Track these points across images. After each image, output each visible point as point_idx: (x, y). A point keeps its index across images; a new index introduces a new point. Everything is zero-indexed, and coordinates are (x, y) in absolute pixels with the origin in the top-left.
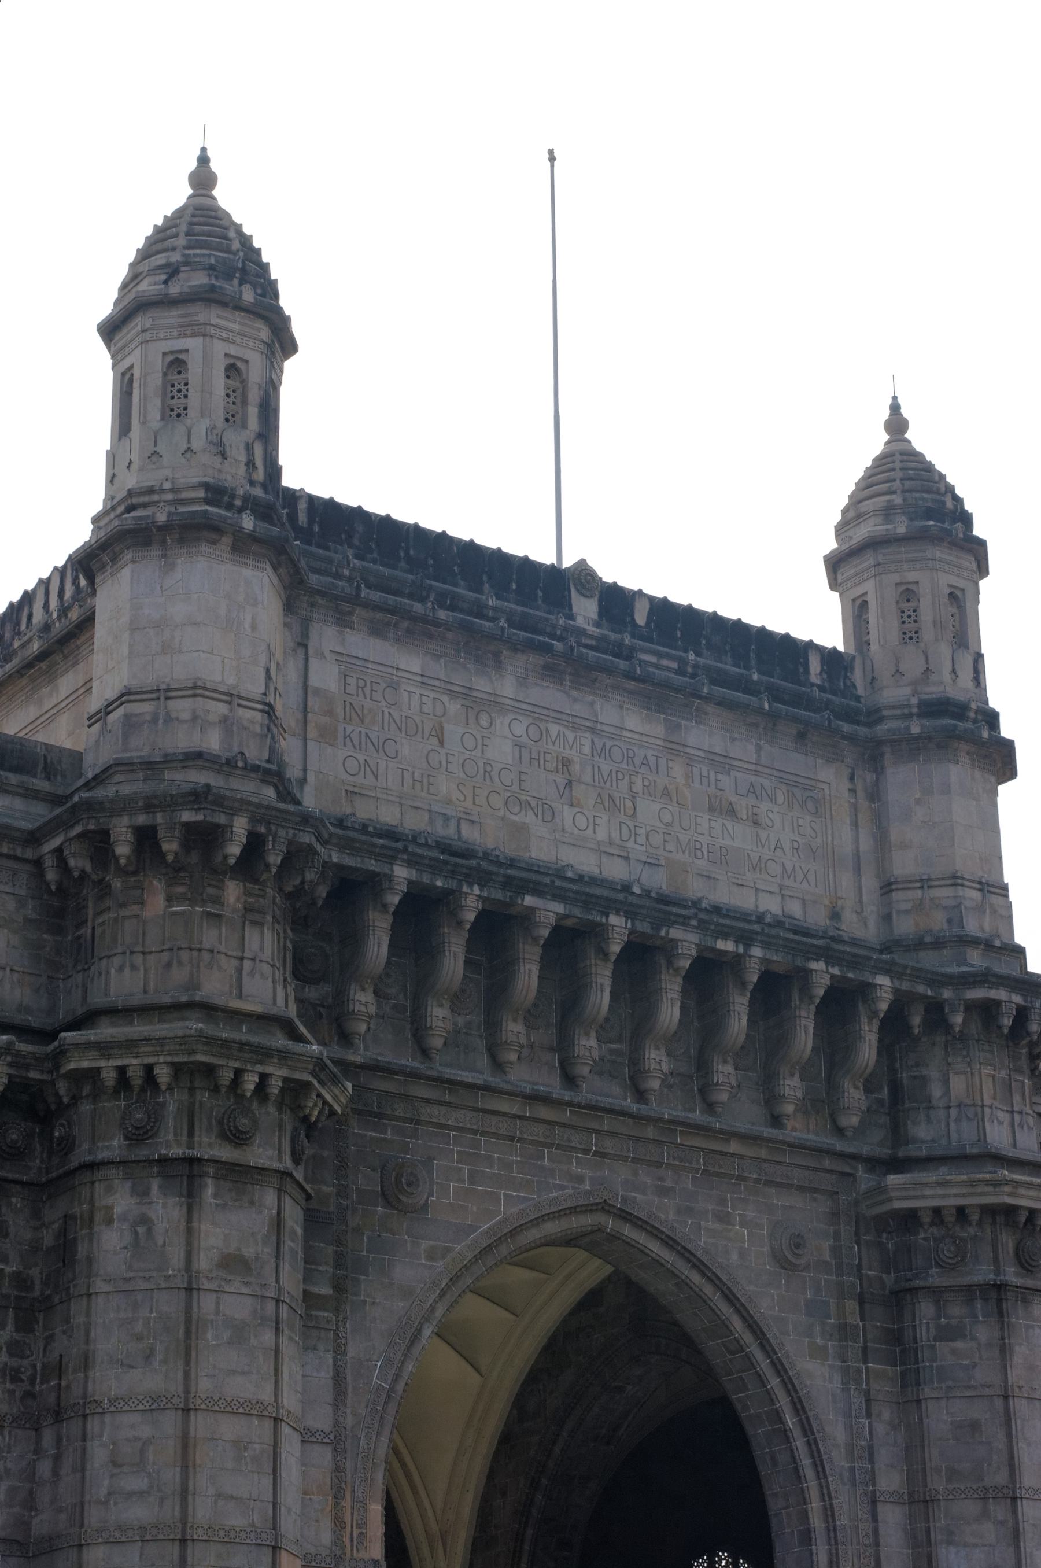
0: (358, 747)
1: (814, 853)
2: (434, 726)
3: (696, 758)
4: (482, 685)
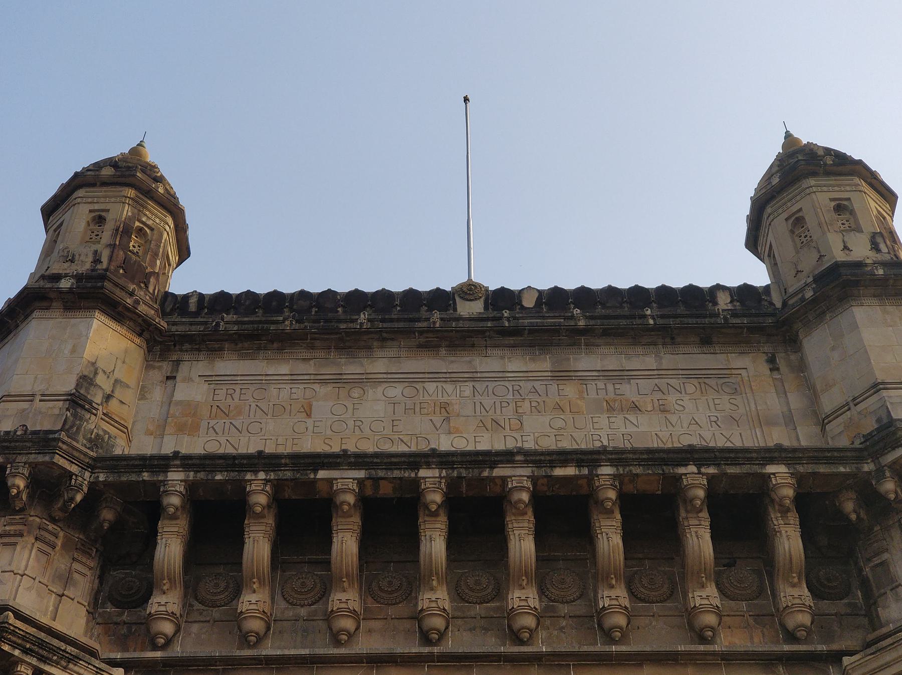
0: (220, 433)
2: (302, 406)
4: (351, 368)
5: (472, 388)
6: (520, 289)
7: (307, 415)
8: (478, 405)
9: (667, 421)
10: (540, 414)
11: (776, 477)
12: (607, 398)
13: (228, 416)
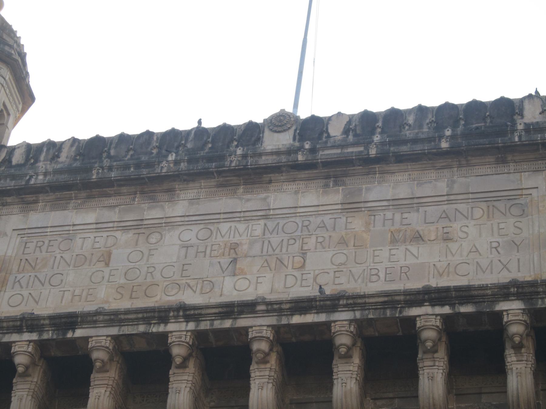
1: (518, 246)
2: (103, 255)
3: (380, 208)
5: (263, 227)
6: (330, 115)
7: (106, 264)
8: (266, 243)
9: (448, 250)
10: (323, 250)
11: (508, 314)
12: (392, 229)
13: (34, 269)
